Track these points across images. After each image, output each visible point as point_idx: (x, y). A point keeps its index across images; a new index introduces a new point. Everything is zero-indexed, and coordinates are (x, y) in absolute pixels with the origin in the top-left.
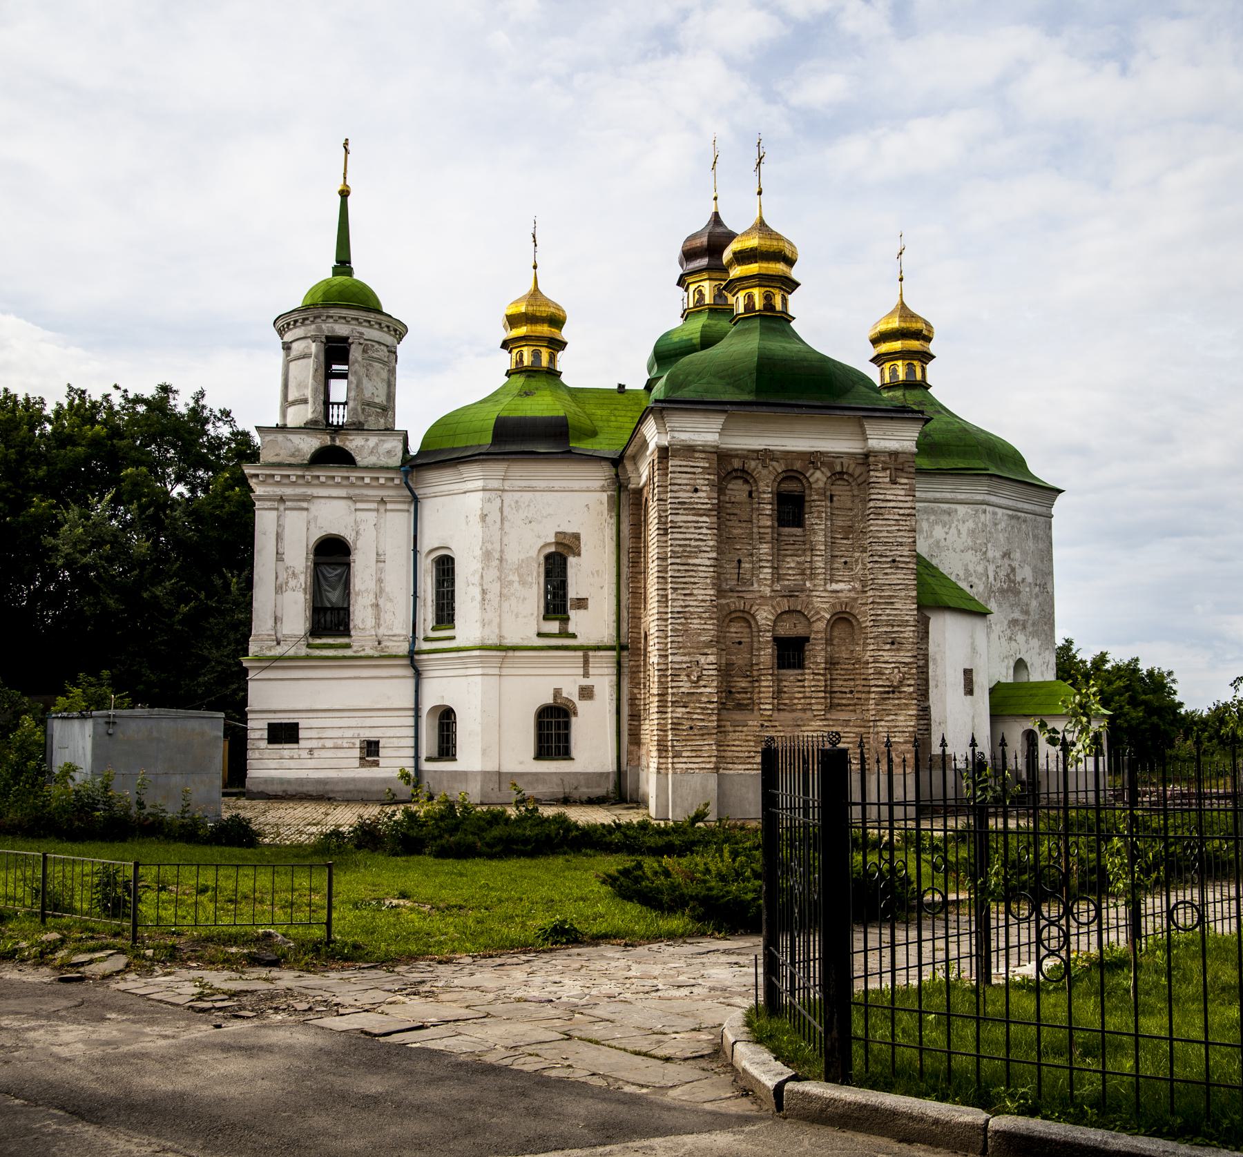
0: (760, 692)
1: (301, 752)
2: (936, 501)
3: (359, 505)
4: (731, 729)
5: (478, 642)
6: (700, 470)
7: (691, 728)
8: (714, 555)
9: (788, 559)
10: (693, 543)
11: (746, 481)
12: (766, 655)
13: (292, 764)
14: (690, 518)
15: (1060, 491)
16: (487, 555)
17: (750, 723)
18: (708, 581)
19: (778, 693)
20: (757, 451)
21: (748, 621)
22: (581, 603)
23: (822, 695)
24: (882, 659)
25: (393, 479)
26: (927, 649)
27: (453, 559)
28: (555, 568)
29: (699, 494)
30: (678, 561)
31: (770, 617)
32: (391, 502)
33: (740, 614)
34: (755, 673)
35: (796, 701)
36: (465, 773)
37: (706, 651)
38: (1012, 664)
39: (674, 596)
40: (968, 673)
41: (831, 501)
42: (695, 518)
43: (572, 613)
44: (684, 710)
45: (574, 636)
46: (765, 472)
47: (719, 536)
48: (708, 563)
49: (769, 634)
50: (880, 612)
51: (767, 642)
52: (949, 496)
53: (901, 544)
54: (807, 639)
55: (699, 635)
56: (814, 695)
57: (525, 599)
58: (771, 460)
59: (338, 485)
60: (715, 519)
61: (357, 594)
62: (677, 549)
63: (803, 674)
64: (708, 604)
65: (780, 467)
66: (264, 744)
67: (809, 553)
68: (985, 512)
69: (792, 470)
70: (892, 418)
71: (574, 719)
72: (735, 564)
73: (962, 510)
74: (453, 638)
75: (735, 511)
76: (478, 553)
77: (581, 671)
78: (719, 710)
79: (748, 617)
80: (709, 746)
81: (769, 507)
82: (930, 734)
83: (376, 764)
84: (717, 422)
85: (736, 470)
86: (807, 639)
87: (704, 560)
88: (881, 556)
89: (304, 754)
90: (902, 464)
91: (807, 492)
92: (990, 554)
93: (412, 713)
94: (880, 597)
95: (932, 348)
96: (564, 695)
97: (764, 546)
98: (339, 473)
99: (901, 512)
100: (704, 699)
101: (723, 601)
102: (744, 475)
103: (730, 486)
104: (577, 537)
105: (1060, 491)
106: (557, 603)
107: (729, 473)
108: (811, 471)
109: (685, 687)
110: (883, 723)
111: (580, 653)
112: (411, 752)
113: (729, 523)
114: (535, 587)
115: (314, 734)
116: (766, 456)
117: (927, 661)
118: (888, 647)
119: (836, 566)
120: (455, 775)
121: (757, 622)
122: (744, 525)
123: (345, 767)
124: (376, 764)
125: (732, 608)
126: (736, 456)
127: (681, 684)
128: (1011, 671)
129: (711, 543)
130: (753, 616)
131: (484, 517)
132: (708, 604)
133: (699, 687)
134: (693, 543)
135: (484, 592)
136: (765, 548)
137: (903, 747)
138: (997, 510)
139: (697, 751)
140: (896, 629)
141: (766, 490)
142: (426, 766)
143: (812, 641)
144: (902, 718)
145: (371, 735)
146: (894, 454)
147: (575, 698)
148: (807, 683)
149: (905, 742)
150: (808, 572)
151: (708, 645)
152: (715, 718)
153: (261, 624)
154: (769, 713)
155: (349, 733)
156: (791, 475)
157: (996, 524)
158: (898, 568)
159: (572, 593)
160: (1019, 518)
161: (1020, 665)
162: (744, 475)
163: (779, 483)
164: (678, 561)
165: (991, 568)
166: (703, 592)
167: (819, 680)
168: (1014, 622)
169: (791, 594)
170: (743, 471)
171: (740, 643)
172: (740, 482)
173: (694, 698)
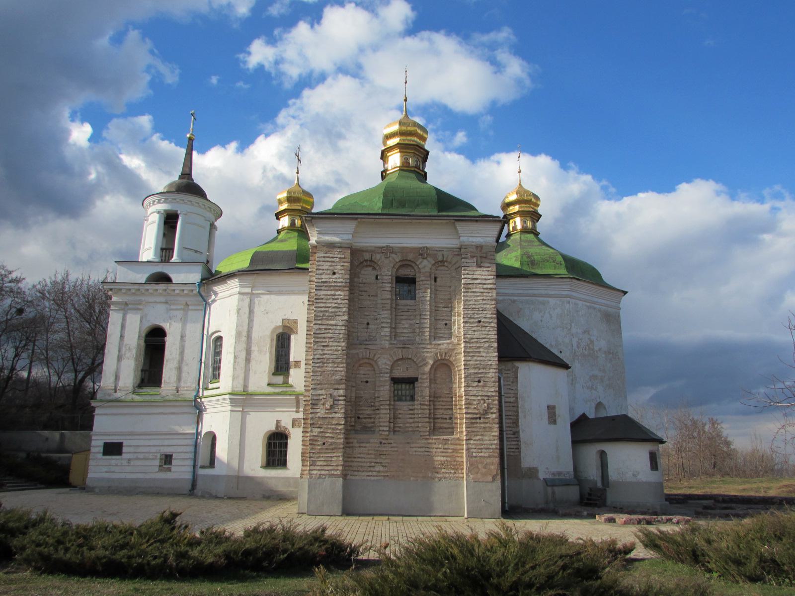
0: (380, 418)
1: (123, 461)
2: (534, 295)
3: (172, 307)
4: (357, 445)
5: (230, 391)
6: (338, 260)
7: (324, 444)
8: (346, 318)
9: (403, 322)
10: (330, 310)
11: (374, 269)
12: (385, 390)
13: (117, 469)
14: (329, 293)
15: (625, 293)
16: (238, 334)
17: (372, 441)
18: (341, 336)
19: (394, 418)
20: (381, 248)
21: (373, 366)
23: (427, 420)
24: (471, 393)
25: (192, 291)
26: (517, 390)
28: (282, 341)
30: (320, 322)
31: (388, 362)
32: (192, 305)
33: (366, 361)
34: (377, 404)
35: (408, 425)
36: (218, 476)
37: (336, 386)
38: (594, 405)
39: (315, 347)
40: (551, 409)
41: (435, 281)
42: (333, 292)
43: (291, 371)
44: (319, 430)
45: (291, 386)
46: (387, 261)
47: (350, 305)
48: (341, 323)
49: (388, 375)
50: (469, 358)
51: (386, 381)
52: (543, 292)
53: (484, 310)
54: (416, 379)
55: (333, 375)
56: (420, 420)
57: (261, 362)
58: (392, 253)
59: (161, 294)
60: (347, 293)
61: (167, 361)
62: (318, 314)
63: (413, 405)
64: (340, 352)
65: (398, 258)
66: (100, 456)
67: (418, 317)
68: (569, 303)
69: (407, 260)
70: (477, 221)
71: (289, 441)
72: (365, 325)
73: (552, 301)
74: (219, 388)
75: (366, 289)
76: (234, 333)
78: (346, 430)
79: (373, 363)
80: (338, 458)
81: (390, 285)
82: (520, 452)
83: (169, 470)
84: (351, 226)
85: (367, 261)
86: (416, 379)
87: (340, 320)
88: (470, 318)
89: (125, 462)
90: (486, 253)
91: (418, 275)
92: (574, 331)
94: (470, 347)
95: (540, 210)
97: (385, 312)
98: (162, 287)
99: (485, 286)
100: (334, 422)
101: (354, 352)
102: (372, 264)
103: (363, 272)
104: (295, 322)
105: (625, 293)
106: (282, 365)
107: (361, 263)
108: (420, 260)
109: (321, 412)
110: (472, 442)
111: (293, 397)
112: (191, 463)
113: (360, 297)
114: (268, 354)
115: (132, 450)
116: (387, 251)
117: (517, 398)
118: (476, 384)
119: (439, 326)
120: (216, 478)
121: (379, 367)
122: (372, 298)
123: (151, 472)
124: (169, 470)
125: (361, 356)
126: (367, 251)
127: (318, 411)
128: (593, 410)
129: (344, 309)
130: (376, 362)
131: (239, 310)
132: (340, 352)
133: (331, 413)
134: (330, 310)
135: (235, 357)
136: (385, 314)
137: (488, 460)
138: (578, 302)
139: (328, 462)
140: (481, 371)
141: (387, 274)
142: (201, 472)
143: (420, 380)
144: (487, 438)
145: (168, 450)
146: (479, 247)
147: (289, 426)
148: (415, 413)
149: (489, 457)
150: (417, 331)
151: (339, 382)
152: (342, 436)
153: (107, 381)
154: (387, 433)
155: (153, 450)
156: (406, 263)
157: (577, 311)
158: (482, 326)
159: (292, 359)
160: (595, 308)
161: (599, 406)
162: (372, 264)
163: (398, 270)
164: (320, 322)
165: (575, 341)
166: (335, 344)
167: (424, 409)
168: (594, 377)
169: (404, 346)
170: (371, 261)
171: (367, 382)
172: (370, 269)
173: (327, 421)
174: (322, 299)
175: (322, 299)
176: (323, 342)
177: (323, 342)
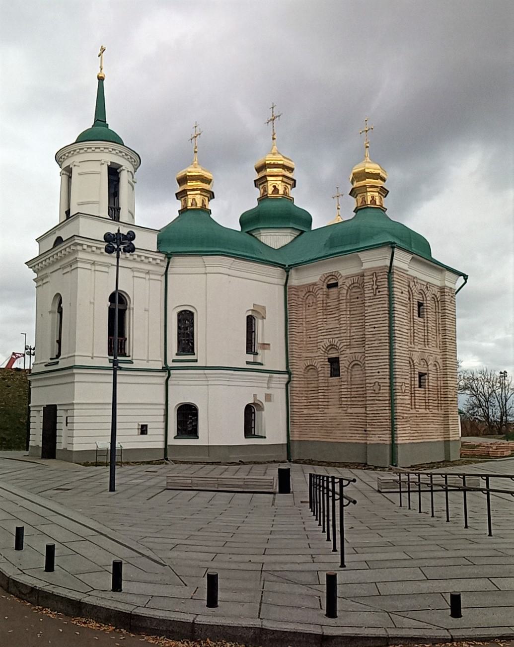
22: (265, 346)
27: (192, 314)
29: (403, 295)
45: (261, 364)
74: (196, 361)
77: (266, 385)
93: (164, 407)
96: (258, 398)
104: (264, 308)
111: (268, 375)
142: (171, 441)
150: (426, 340)
159: (259, 339)
174: (397, 311)
175: (397, 311)
176: (400, 343)
177: (400, 343)
